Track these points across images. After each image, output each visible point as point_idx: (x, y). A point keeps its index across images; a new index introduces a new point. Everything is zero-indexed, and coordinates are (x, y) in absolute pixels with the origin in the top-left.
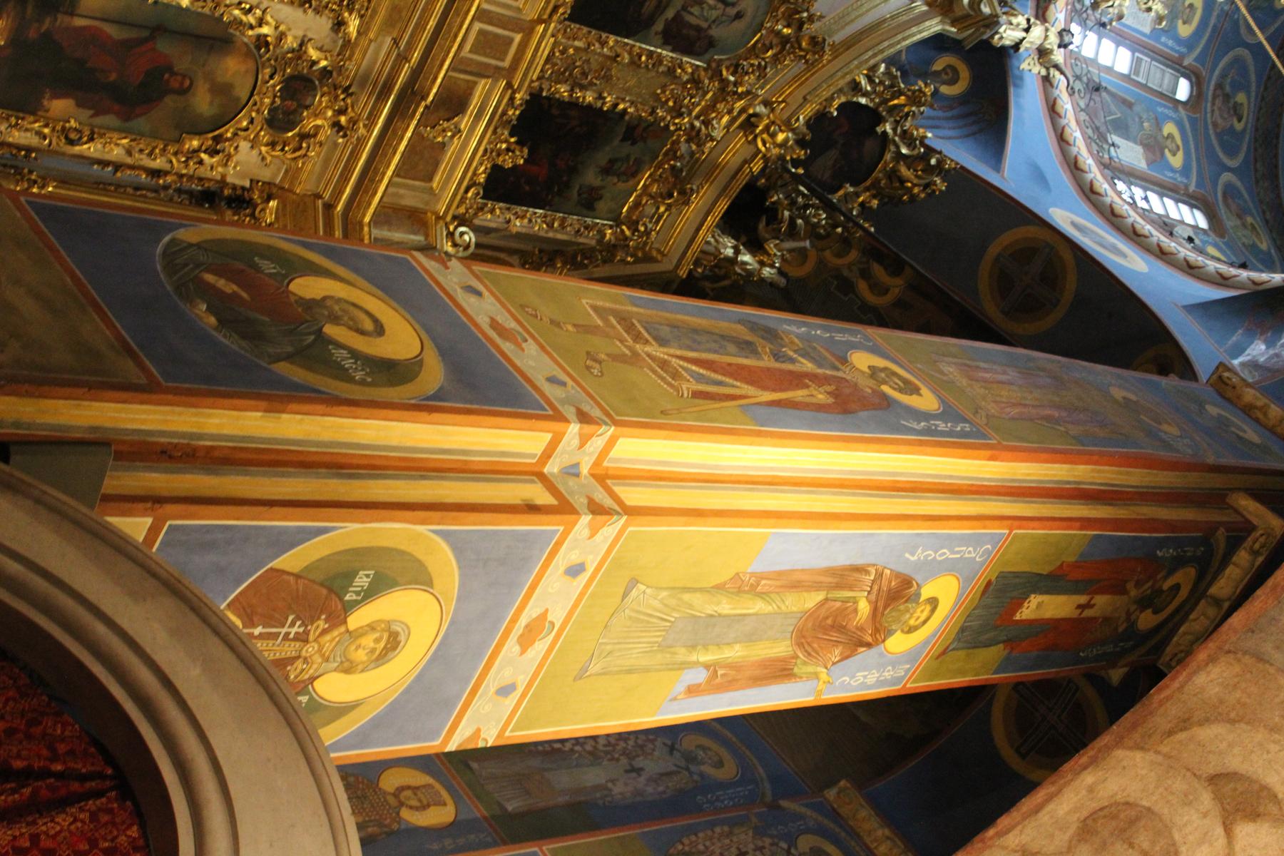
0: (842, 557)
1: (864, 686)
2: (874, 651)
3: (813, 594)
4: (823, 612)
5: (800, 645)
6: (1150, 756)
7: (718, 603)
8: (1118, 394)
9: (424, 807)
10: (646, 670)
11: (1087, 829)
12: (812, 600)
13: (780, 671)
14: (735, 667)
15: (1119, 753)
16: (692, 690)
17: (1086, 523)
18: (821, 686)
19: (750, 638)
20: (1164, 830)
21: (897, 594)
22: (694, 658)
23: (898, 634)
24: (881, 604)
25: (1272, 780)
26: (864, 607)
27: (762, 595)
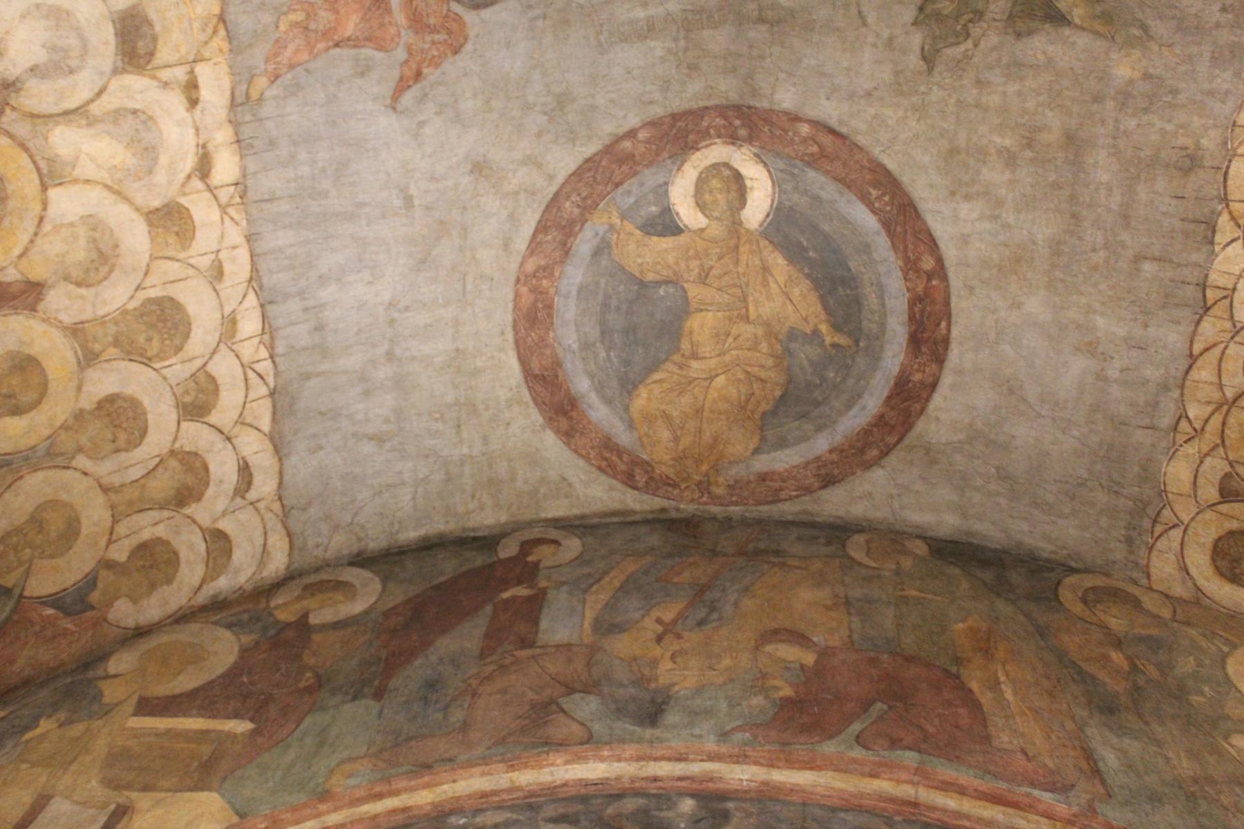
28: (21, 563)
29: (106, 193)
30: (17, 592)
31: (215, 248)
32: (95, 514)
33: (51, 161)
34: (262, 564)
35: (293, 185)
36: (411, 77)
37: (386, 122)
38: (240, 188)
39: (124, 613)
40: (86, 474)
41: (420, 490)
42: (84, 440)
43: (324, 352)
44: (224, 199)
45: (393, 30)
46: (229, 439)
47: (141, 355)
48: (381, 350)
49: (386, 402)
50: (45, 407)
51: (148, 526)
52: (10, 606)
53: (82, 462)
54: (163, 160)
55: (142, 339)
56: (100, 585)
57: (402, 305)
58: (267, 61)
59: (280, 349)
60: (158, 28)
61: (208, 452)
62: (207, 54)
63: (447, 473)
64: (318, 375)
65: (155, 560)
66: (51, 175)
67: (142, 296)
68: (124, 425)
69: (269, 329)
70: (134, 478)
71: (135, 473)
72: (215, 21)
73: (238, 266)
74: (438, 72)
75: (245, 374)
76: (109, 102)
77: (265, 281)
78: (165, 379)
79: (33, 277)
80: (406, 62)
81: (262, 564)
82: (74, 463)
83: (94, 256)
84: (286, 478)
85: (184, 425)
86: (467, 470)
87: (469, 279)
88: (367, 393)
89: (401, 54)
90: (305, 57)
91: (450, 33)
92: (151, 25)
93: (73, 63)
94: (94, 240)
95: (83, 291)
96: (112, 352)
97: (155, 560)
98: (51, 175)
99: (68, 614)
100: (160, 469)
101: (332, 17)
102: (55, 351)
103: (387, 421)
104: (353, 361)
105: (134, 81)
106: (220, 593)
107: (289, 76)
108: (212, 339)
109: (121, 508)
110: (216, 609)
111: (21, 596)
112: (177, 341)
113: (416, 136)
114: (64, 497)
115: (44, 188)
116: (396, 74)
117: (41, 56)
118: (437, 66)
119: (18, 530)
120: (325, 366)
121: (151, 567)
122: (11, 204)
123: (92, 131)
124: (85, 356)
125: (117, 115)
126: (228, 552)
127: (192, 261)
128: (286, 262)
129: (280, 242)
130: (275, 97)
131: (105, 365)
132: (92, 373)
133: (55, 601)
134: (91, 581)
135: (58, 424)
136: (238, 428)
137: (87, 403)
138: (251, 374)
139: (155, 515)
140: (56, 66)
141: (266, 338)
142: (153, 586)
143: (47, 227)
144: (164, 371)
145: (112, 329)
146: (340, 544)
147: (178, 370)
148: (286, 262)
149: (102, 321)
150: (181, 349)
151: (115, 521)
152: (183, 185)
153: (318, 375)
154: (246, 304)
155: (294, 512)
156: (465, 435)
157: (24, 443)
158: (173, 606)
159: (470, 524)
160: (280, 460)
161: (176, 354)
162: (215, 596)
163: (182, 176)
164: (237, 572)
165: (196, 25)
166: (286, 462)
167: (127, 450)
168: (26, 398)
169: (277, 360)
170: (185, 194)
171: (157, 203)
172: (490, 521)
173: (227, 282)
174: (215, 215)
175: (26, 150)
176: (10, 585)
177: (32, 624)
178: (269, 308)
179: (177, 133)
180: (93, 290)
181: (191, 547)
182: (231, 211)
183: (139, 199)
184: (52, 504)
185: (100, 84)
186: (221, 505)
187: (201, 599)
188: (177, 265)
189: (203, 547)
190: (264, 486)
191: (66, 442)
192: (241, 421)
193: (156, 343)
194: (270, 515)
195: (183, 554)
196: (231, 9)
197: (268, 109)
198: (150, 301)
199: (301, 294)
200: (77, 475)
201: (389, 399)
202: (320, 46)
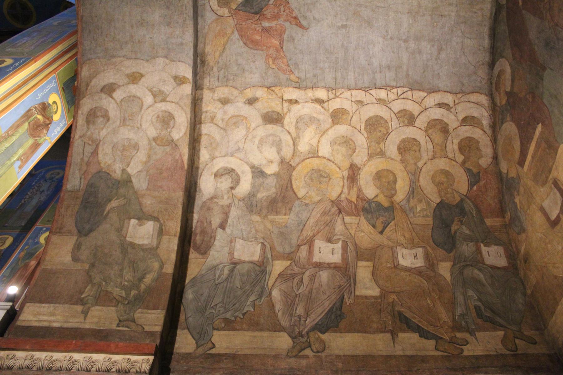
0: (22, 111)
1: (59, 132)
2: (52, 124)
3: (24, 125)
4: (31, 126)
5: (34, 137)
6: (87, 97)
7: (4, 145)
8: (55, 23)
9: (5, 242)
10: (4, 173)
11: (88, 122)
12: (26, 126)
13: (36, 146)
14: (23, 155)
15: (81, 102)
16: (20, 167)
17: (71, 58)
18: (49, 141)
19: (21, 146)
20: (101, 109)
21: (44, 108)
22: (12, 161)
23: (54, 115)
24: (43, 113)
25: (112, 81)
26: (40, 117)
27: (12, 135)
28: (453, 193)
29: (324, 137)
30: (463, 197)
31: (350, 102)
32: (442, 164)
33: (309, 152)
34: (482, 105)
35: (331, 70)
36: (296, 21)
37: (313, 33)
38: (330, 90)
39: (485, 161)
40: (425, 164)
41: (467, 35)
42: (412, 162)
43: (399, 67)
44: (333, 96)
45: (278, 26)
46: (426, 109)
47: (385, 135)
48: (403, 44)
49: (425, 45)
50: (396, 172)
51: (453, 146)
52: (467, 200)
53: (420, 164)
54: (315, 115)
55: (379, 134)
56: (471, 168)
57: (385, 34)
58: (285, 74)
59: (394, 84)
60: (270, 110)
62: (280, 95)
63: (462, 23)
64: (408, 71)
66: (314, 154)
67: (363, 131)
68: (410, 146)
71: (430, 146)
72: (269, 90)
73: (359, 95)
74: (295, 10)
75: (401, 99)
76: (292, 130)
77: (366, 86)
78: (396, 128)
79: (348, 166)
80: (290, 22)
81: (482, 105)
82: (420, 167)
83: (345, 145)
84: (448, 90)
85: (416, 125)
86: (463, 14)
87: (379, 5)
88: (420, 52)
89: (287, 24)
90: (285, 60)
91: (281, 5)
92: (268, 112)
93: (278, 140)
94: (340, 143)
95: (357, 151)
96: (382, 145)
97: (468, 146)
98: (314, 154)
99: (478, 182)
100: (431, 137)
101: (272, 49)
102: (377, 164)
103: (433, 46)
104: (405, 56)
105: (287, 121)
106: (489, 124)
107: (291, 66)
109: (443, 154)
110: (495, 127)
111: (465, 196)
112: (383, 122)
113: (319, 21)
114: (432, 173)
115: (318, 157)
116: (294, 26)
117: (274, 150)
118: (293, 10)
119: (439, 191)
120: (405, 68)
121: (470, 148)
122: (321, 168)
123: (301, 137)
124: (381, 155)
125: (297, 128)
126: (473, 118)
127: (354, 111)
128: (361, 77)
129: (353, 78)
130: (298, 73)
131: (386, 148)
132: (388, 154)
134: (468, 171)
135: (404, 169)
136: (422, 105)
137: (398, 158)
139: (449, 142)
140: (278, 145)
141: (388, 89)
142: (478, 149)
143: (332, 158)
144: (393, 128)
145: (373, 143)
146: (482, 73)
147: (394, 123)
148: (361, 77)
149: (369, 147)
151: (447, 157)
152: (325, 110)
153: (408, 71)
154: (374, 94)
155: (463, 89)
156: (446, 13)
157: (407, 182)
158: (489, 143)
159: (489, 15)
160: (439, 91)
161: (387, 123)
162: (490, 126)
163: (322, 110)
164: (482, 116)
165: (270, 97)
166: (441, 89)
167: (421, 147)
168: (391, 178)
169: (398, 86)
170: (329, 110)
171: (330, 120)
172: (489, 6)
173: (364, 100)
174: (338, 100)
175: (304, 160)
176: (459, 199)
179: (307, 109)
180: (357, 147)
181: (467, 131)
182: (338, 94)
183: (328, 126)
184: (433, 178)
185: (286, 132)
186: (452, 117)
187: (489, 132)
188: (354, 117)
189: (467, 127)
190: (449, 99)
191: (411, 168)
192: (420, 104)
193: (382, 129)
194: (462, 99)
196: (266, 84)
197: (302, 76)
198: (366, 128)
199: (374, 73)
200: (425, 166)
201: (424, 44)
202: (282, 54)
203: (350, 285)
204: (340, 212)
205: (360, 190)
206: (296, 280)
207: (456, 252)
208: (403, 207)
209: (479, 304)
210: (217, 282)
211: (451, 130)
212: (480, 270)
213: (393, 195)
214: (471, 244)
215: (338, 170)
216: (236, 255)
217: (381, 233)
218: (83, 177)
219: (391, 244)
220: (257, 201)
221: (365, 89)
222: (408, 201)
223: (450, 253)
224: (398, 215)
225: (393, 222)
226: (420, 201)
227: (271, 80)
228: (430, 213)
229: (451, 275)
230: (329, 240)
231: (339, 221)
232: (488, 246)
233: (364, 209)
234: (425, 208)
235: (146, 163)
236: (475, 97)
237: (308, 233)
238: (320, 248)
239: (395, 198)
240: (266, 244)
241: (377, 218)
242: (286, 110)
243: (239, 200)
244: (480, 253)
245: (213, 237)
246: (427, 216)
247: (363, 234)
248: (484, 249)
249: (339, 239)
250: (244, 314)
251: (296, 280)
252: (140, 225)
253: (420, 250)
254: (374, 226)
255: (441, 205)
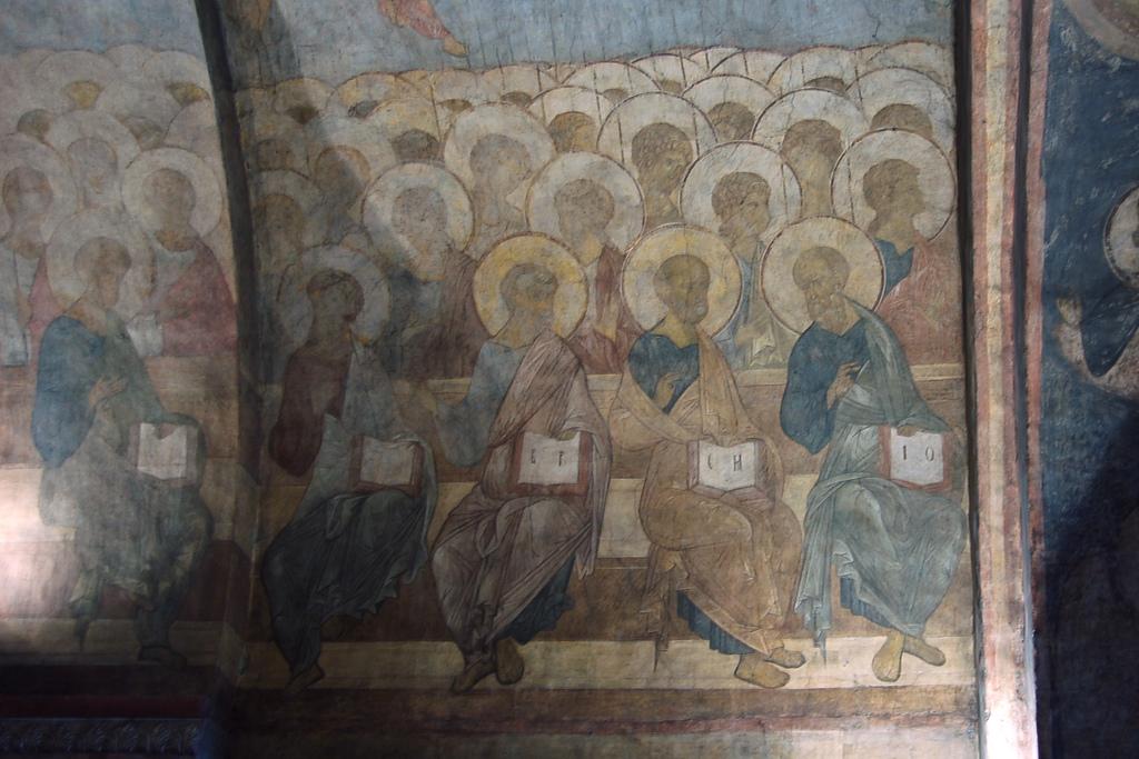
28: (842, 305)
30: (866, 314)
31: (594, 95)
32: (821, 232)
35: (540, 19)
38: (542, 68)
40: (780, 234)
50: (708, 261)
51: (849, 186)
53: (767, 236)
61: (790, 118)
65: (887, 184)
68: (744, 193)
69: (682, 49)
70: (798, 191)
72: (399, 80)
73: (614, 74)
76: (467, 174)
77: (630, 51)
79: (597, 253)
84: (838, 41)
96: (674, 196)
105: (450, 152)
107: (443, 17)
108: (678, 103)
109: (823, 208)
111: (871, 311)
119: (809, 303)
124: (673, 220)
127: (604, 117)
131: (684, 204)
133: (888, 285)
134: (884, 247)
138: (718, 70)
139: (840, 178)
141: (686, 53)
144: (701, 152)
150: (683, 134)
151: (834, 215)
160: (816, 46)
161: (688, 140)
166: (819, 41)
168: (697, 273)
169: (707, 44)
171: (549, 145)
175: (498, 243)
176: (856, 319)
177: (903, 306)
178: (655, 50)
181: (885, 146)
183: (548, 158)
184: (796, 271)
188: (606, 130)
189: (889, 133)
192: (766, 84)
194: (876, 61)
195: (891, 155)
196: (390, 66)
203: (590, 534)
204: (580, 364)
205: (625, 311)
206: (483, 527)
207: (830, 450)
208: (720, 346)
209: (853, 574)
210: (330, 535)
211: (846, 146)
212: (876, 494)
213: (699, 319)
214: (867, 430)
215: (574, 263)
216: (365, 476)
217: (667, 410)
218: (28, 332)
219: (686, 436)
220: (402, 347)
221: (626, 60)
222: (734, 330)
223: (817, 452)
224: (707, 361)
225: (696, 383)
226: (761, 330)
227: (400, 54)
228: (782, 357)
229: (809, 505)
230: (554, 433)
231: (577, 385)
232: (909, 434)
233: (633, 356)
234: (772, 344)
235: (151, 292)
236: (912, 54)
237: (510, 416)
238: (533, 451)
239: (703, 324)
240: (424, 445)
241: (660, 376)
242: (444, 127)
243: (366, 346)
244: (887, 453)
245: (318, 436)
246: (775, 365)
247: (627, 415)
248: (897, 441)
249: (574, 429)
250: (379, 606)
251: (483, 527)
252: (160, 437)
253: (750, 446)
254: (652, 395)
255: (809, 336)
